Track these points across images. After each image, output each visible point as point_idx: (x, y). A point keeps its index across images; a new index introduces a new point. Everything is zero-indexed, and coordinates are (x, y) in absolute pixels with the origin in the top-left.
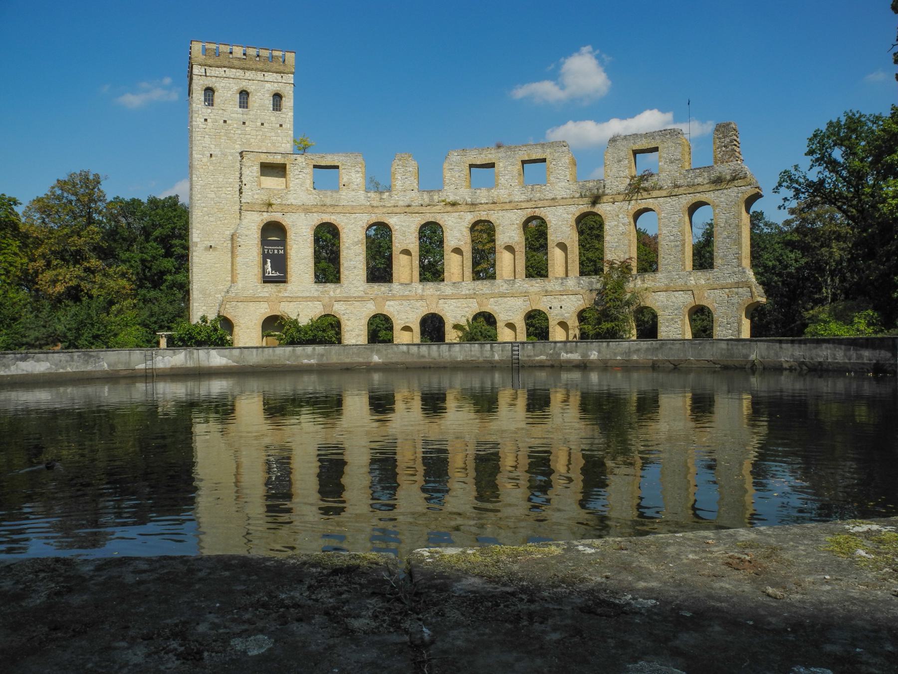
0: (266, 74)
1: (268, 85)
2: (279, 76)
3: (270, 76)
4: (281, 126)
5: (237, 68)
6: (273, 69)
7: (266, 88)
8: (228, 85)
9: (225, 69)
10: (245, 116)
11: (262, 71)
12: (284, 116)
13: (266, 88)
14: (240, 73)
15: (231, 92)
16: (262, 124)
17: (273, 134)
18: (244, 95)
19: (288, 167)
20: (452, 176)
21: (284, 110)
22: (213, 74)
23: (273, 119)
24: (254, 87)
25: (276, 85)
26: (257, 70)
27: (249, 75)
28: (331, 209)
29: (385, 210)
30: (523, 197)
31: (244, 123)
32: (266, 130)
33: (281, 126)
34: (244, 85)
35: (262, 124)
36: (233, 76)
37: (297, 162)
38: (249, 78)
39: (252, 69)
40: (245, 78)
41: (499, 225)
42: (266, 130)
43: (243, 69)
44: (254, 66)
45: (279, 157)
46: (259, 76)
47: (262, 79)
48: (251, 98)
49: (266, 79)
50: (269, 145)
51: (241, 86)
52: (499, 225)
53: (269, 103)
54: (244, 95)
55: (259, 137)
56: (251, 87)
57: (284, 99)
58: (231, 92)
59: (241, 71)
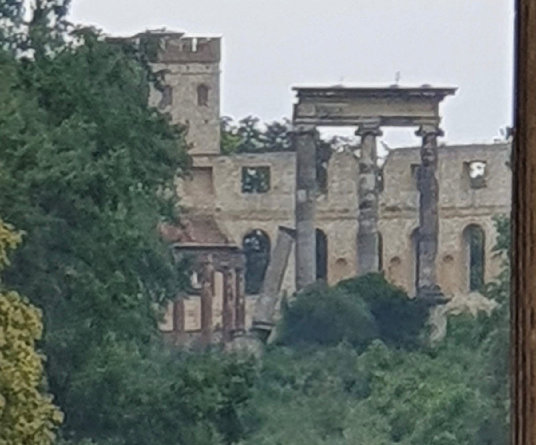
0: (191, 65)
1: (191, 77)
2: (203, 66)
3: (195, 68)
4: (206, 121)
19: (215, 170)
20: (393, 178)
21: (208, 104)
23: (198, 114)
25: (200, 77)
28: (260, 216)
30: (464, 204)
33: (206, 121)
37: (223, 164)
44: (176, 58)
45: (205, 159)
46: (184, 68)
48: (175, 94)
49: (191, 70)
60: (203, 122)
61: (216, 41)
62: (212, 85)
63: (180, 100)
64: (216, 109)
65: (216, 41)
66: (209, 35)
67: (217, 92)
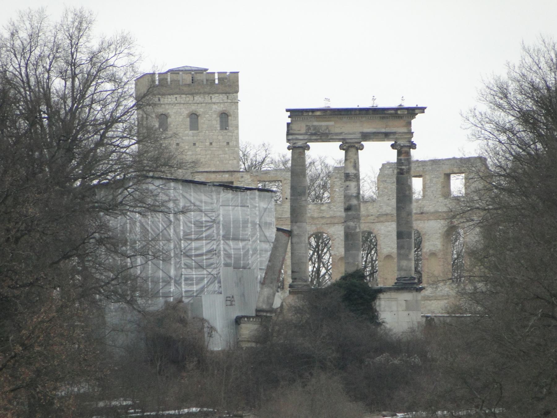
1: (215, 107)
3: (216, 98)
4: (228, 143)
5: (186, 94)
6: (220, 91)
7: (213, 109)
8: (179, 110)
9: (176, 96)
10: (195, 138)
11: (209, 94)
12: (230, 134)
13: (213, 109)
14: (189, 98)
15: (182, 117)
16: (211, 144)
17: (221, 152)
18: (194, 117)
20: (385, 188)
21: (230, 128)
22: (166, 102)
23: (220, 138)
24: (202, 110)
25: (222, 106)
26: (205, 93)
27: (198, 98)
29: (324, 221)
31: (194, 144)
32: (215, 149)
34: (193, 108)
35: (211, 144)
36: (183, 102)
37: (243, 179)
38: (198, 102)
39: (200, 93)
40: (194, 102)
41: (425, 234)
42: (215, 149)
43: (192, 94)
46: (207, 99)
47: (210, 101)
48: (201, 120)
49: (214, 100)
50: (218, 162)
51: (191, 110)
52: (425, 234)
53: (216, 123)
54: (194, 117)
55: (208, 156)
56: (200, 110)
57: (230, 118)
58: (182, 117)
59: (190, 97)
60: (225, 144)
61: (235, 74)
62: (231, 113)
63: (205, 126)
64: (236, 132)
65: (235, 74)
66: (228, 69)
67: (236, 117)
